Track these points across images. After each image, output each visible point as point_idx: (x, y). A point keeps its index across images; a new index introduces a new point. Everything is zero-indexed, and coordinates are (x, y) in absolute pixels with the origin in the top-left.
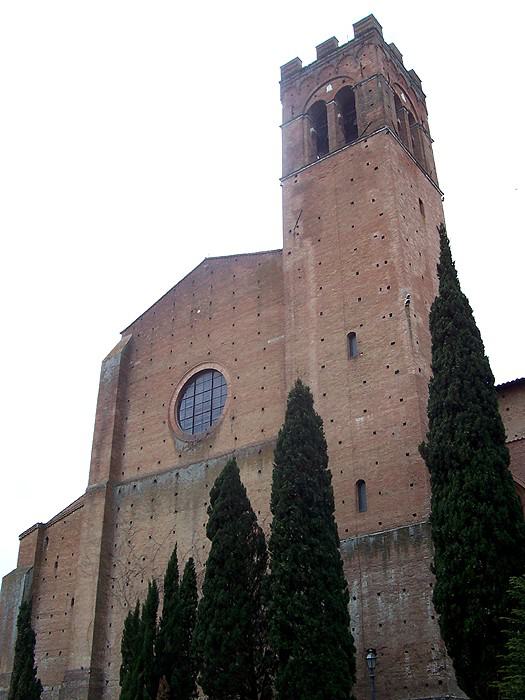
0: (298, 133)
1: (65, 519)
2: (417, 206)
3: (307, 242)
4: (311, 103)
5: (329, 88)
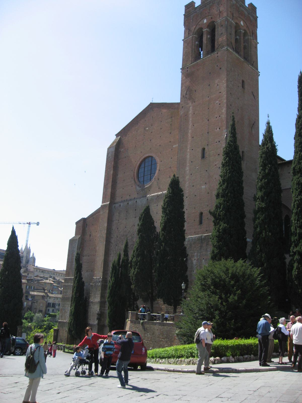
1: (94, 217)
2: (240, 85)
4: (197, 28)
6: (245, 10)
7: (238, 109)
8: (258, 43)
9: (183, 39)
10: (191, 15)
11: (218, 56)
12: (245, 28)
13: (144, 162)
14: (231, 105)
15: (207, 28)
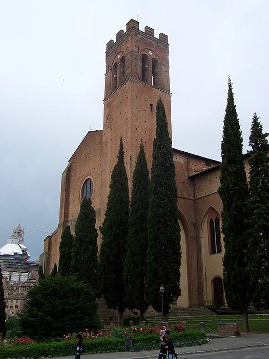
0: (109, 78)
4: (114, 64)
12: (154, 57)
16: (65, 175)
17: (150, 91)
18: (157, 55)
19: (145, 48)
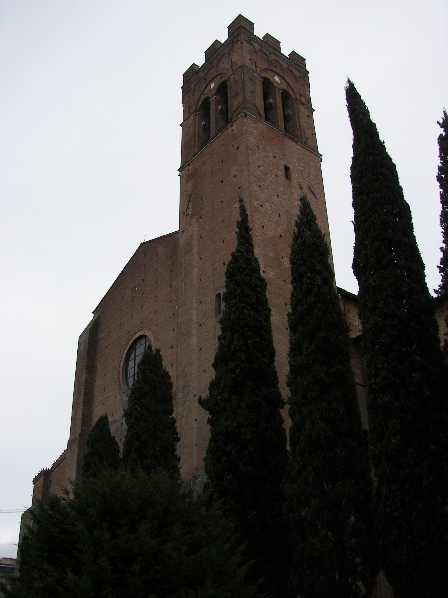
3: (194, 221)
4: (201, 101)
5: (213, 85)
6: (282, 60)
7: (280, 215)
8: (314, 110)
9: (181, 122)
10: (192, 83)
11: (232, 131)
12: (284, 86)
13: (134, 349)
14: (262, 206)
15: (215, 95)
16: (86, 337)
17: (282, 143)
18: (288, 85)
19: (266, 67)
